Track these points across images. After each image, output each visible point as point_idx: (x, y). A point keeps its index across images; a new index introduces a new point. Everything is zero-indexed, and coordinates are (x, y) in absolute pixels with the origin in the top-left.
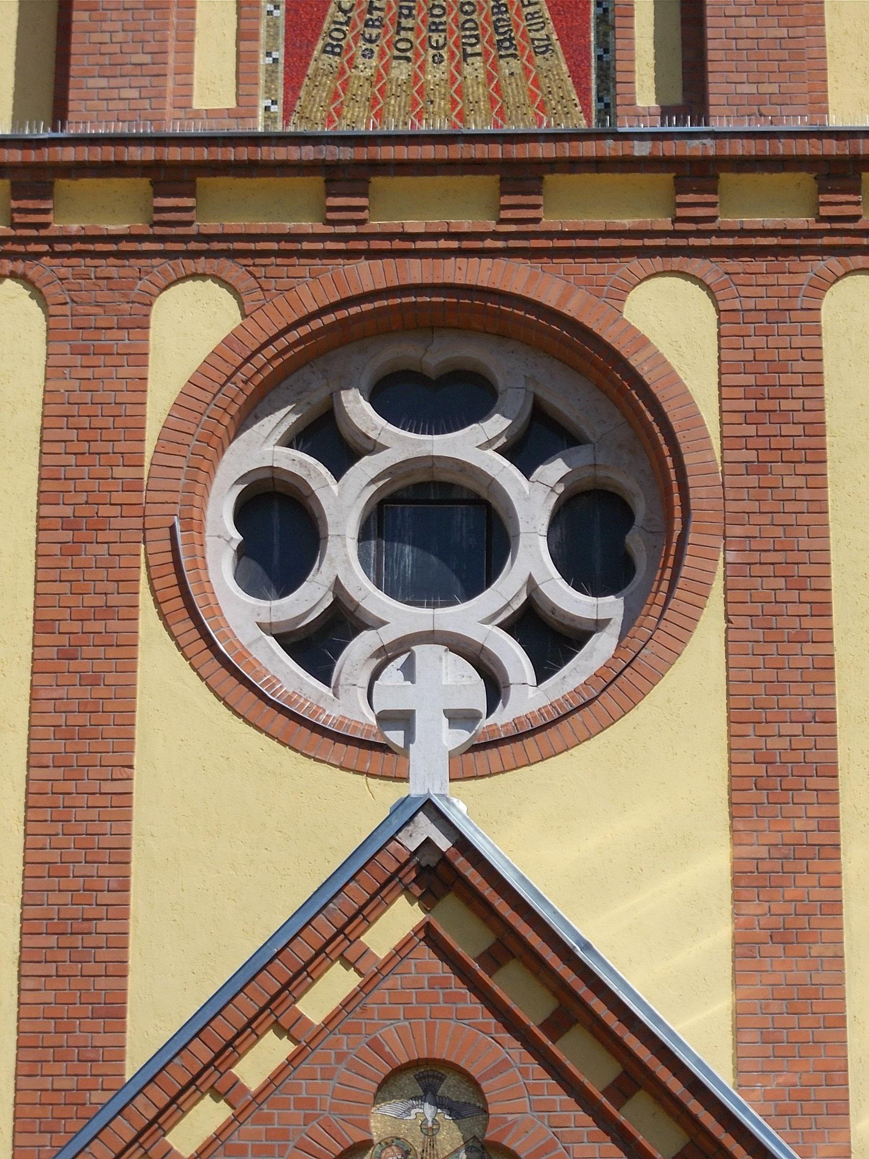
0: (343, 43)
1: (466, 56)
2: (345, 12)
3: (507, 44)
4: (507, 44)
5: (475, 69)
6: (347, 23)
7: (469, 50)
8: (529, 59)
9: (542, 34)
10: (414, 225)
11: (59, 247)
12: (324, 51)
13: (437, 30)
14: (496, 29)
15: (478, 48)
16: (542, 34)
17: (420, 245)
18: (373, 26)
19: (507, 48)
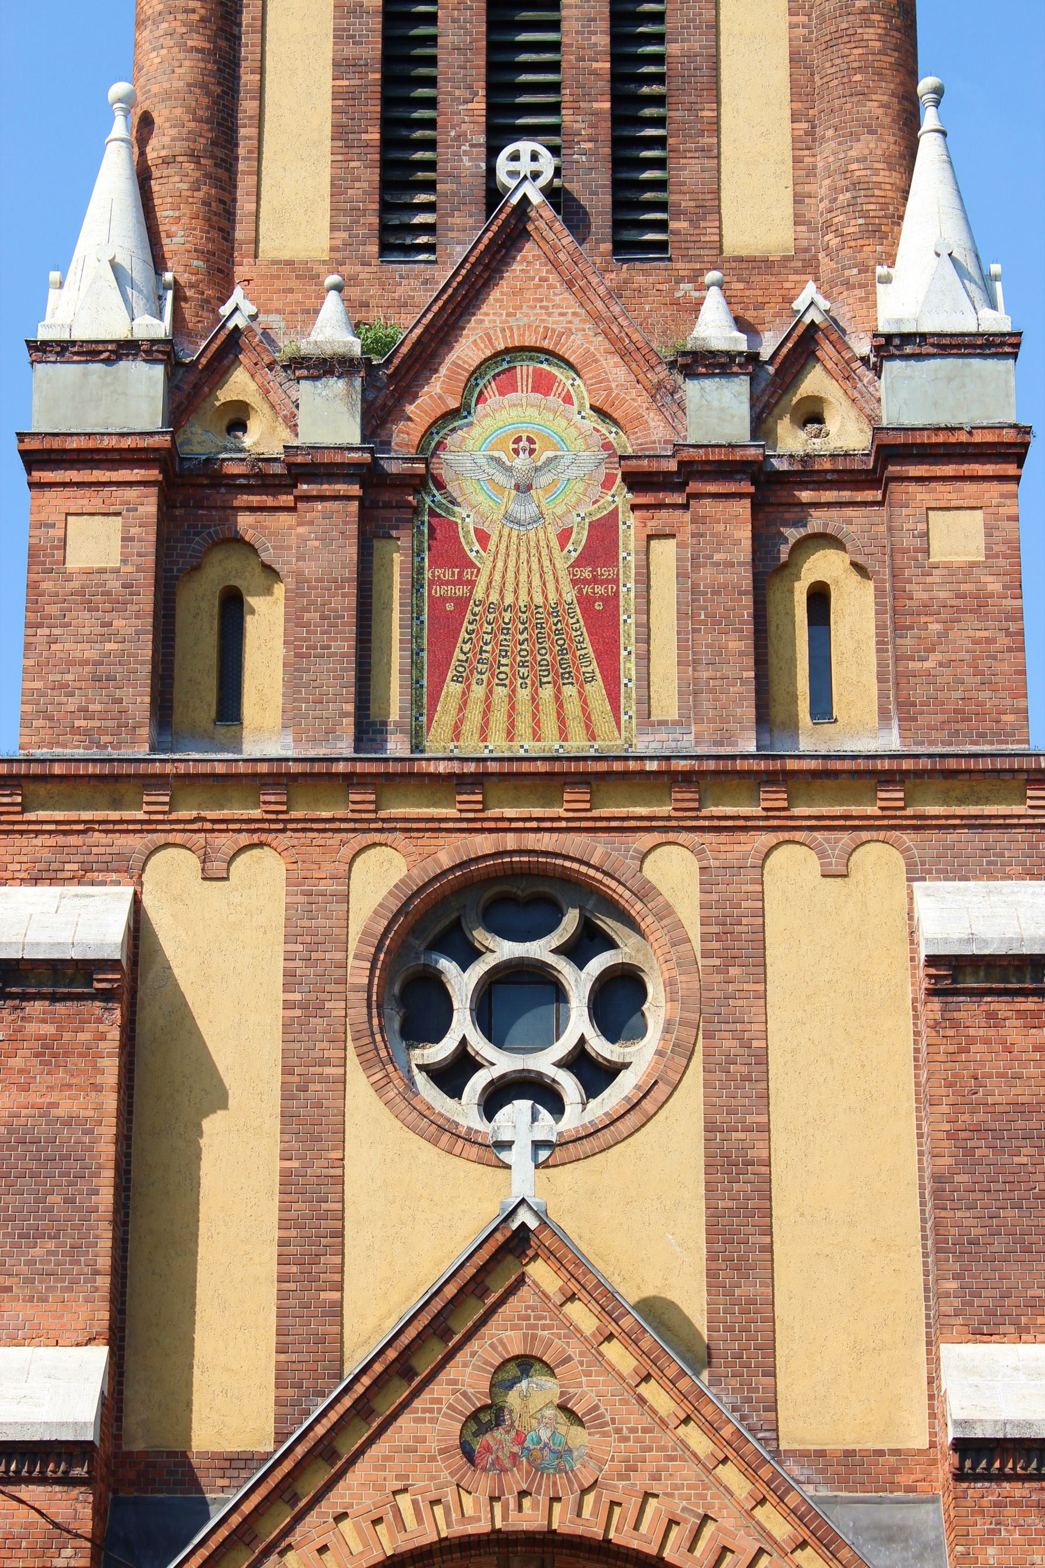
0: (464, 674)
1: (541, 683)
2: (465, 654)
3: (567, 676)
4: (567, 676)
5: (547, 693)
6: (466, 661)
7: (544, 680)
8: (582, 686)
9: (589, 669)
10: (510, 812)
11: (290, 826)
12: (453, 680)
13: (523, 666)
14: (561, 665)
15: (549, 679)
16: (589, 669)
17: (514, 825)
18: (483, 663)
19: (568, 678)
